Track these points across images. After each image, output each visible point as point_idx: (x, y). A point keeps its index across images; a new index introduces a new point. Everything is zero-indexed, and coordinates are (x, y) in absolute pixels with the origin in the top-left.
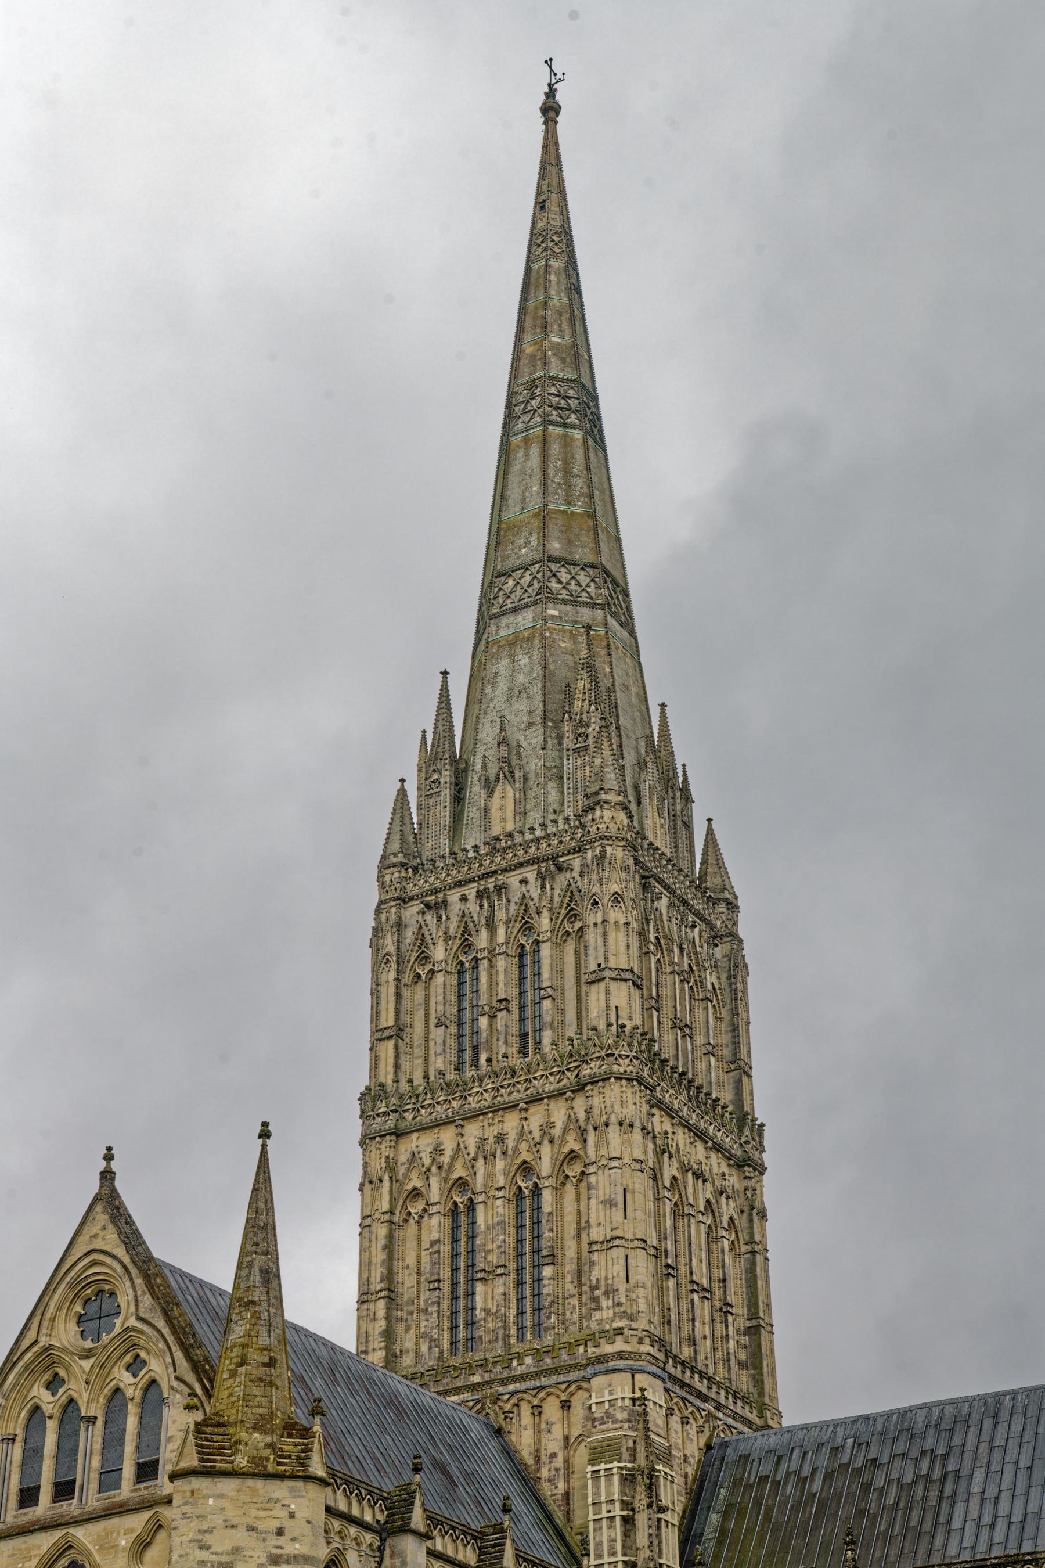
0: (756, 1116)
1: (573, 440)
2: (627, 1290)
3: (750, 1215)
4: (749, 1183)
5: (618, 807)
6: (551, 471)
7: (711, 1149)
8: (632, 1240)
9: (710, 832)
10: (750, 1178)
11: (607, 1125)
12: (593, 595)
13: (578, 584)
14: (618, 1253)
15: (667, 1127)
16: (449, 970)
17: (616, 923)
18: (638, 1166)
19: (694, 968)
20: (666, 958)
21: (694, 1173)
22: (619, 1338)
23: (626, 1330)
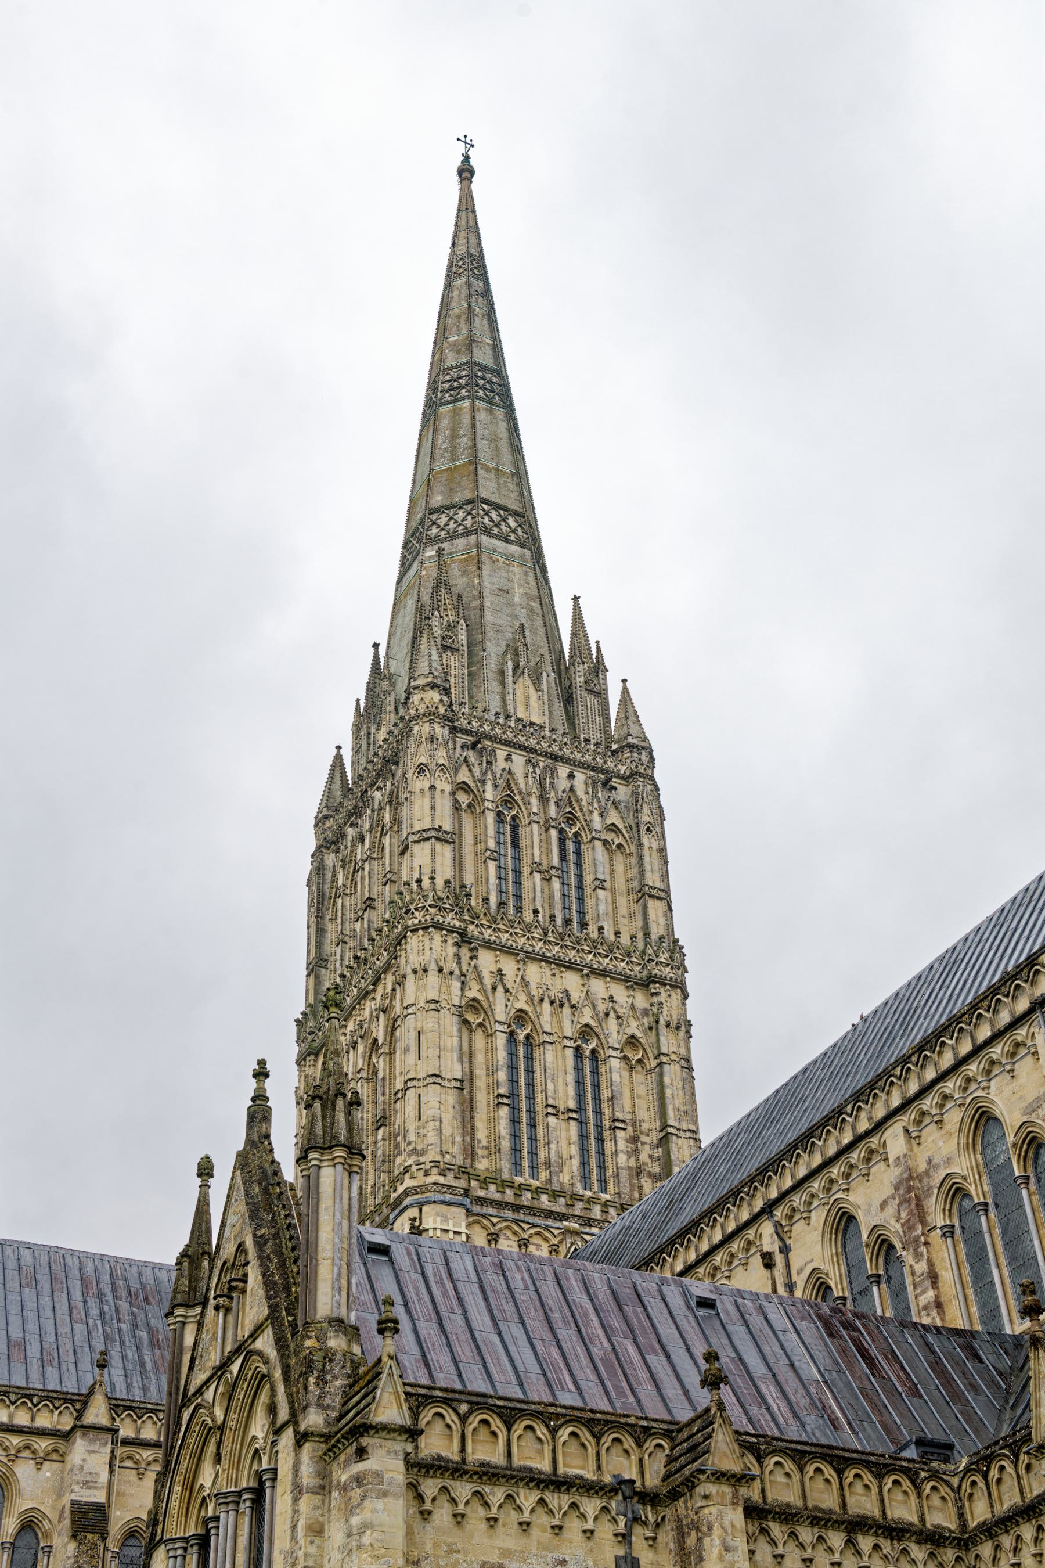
0: (676, 936)
1: (461, 409)
2: (418, 1128)
3: (657, 1029)
4: (655, 999)
5: (427, 688)
6: (439, 442)
7: (587, 975)
8: (424, 1079)
9: (625, 691)
10: (657, 994)
11: (404, 977)
12: (468, 526)
13: (456, 522)
14: (411, 1094)
15: (509, 966)
16: (348, 891)
17: (422, 790)
18: (433, 1006)
19: (579, 814)
20: (525, 812)
21: (552, 1002)
22: (407, 1176)
23: (414, 1168)
